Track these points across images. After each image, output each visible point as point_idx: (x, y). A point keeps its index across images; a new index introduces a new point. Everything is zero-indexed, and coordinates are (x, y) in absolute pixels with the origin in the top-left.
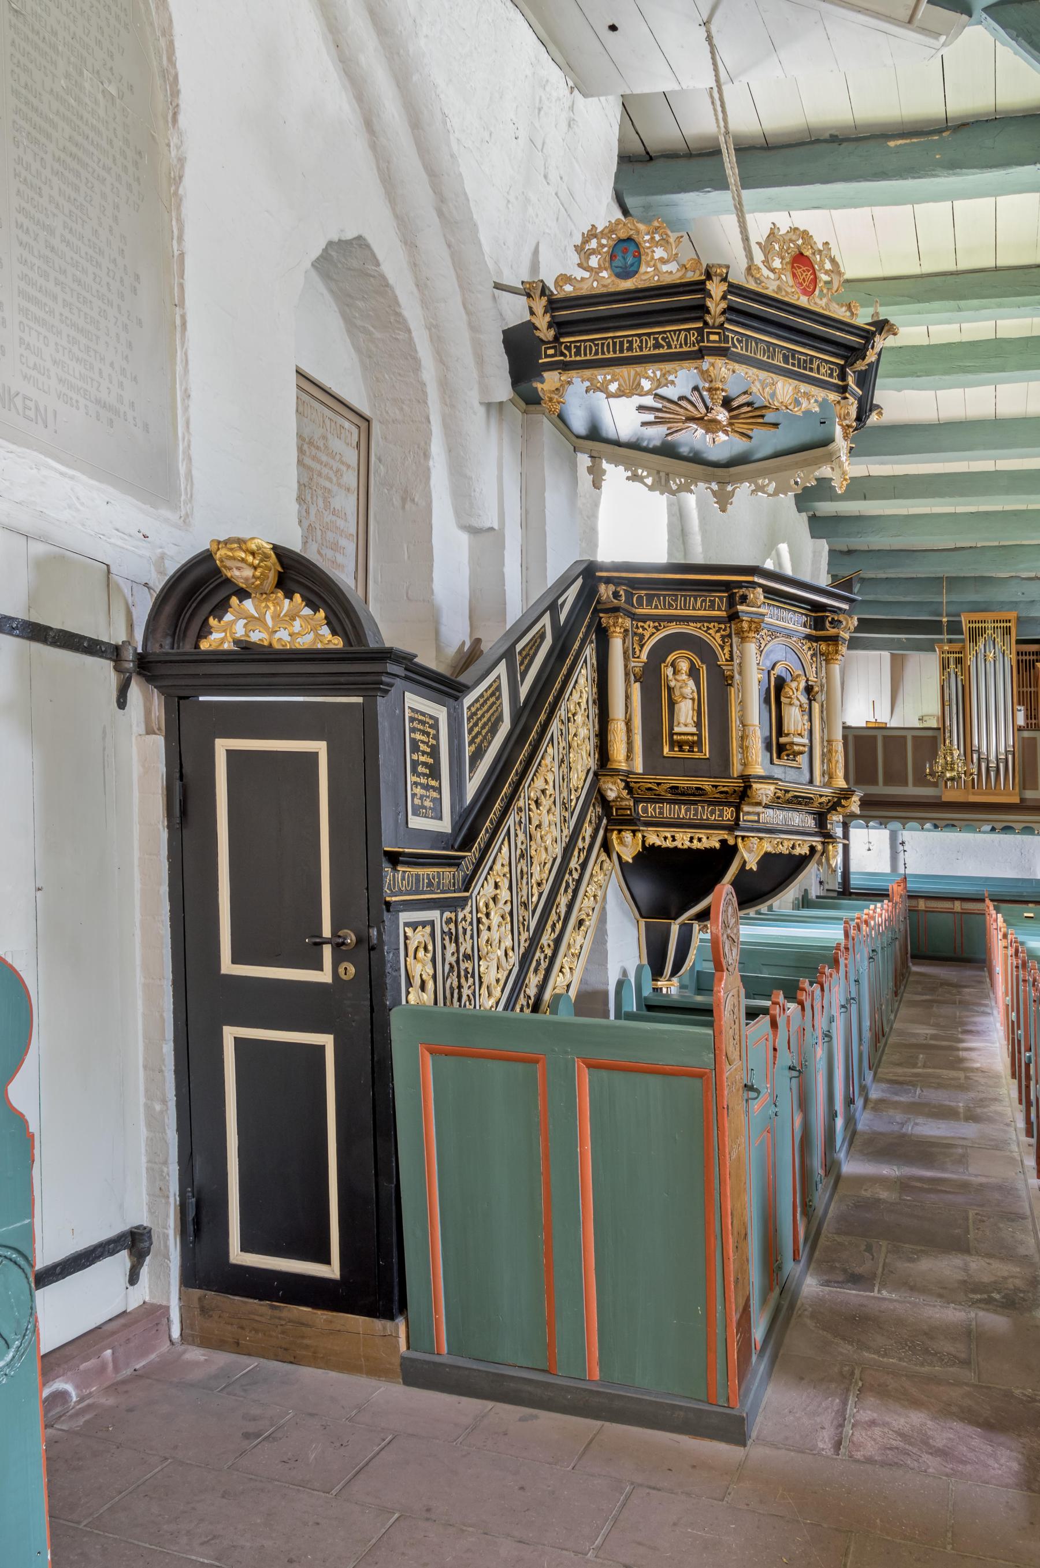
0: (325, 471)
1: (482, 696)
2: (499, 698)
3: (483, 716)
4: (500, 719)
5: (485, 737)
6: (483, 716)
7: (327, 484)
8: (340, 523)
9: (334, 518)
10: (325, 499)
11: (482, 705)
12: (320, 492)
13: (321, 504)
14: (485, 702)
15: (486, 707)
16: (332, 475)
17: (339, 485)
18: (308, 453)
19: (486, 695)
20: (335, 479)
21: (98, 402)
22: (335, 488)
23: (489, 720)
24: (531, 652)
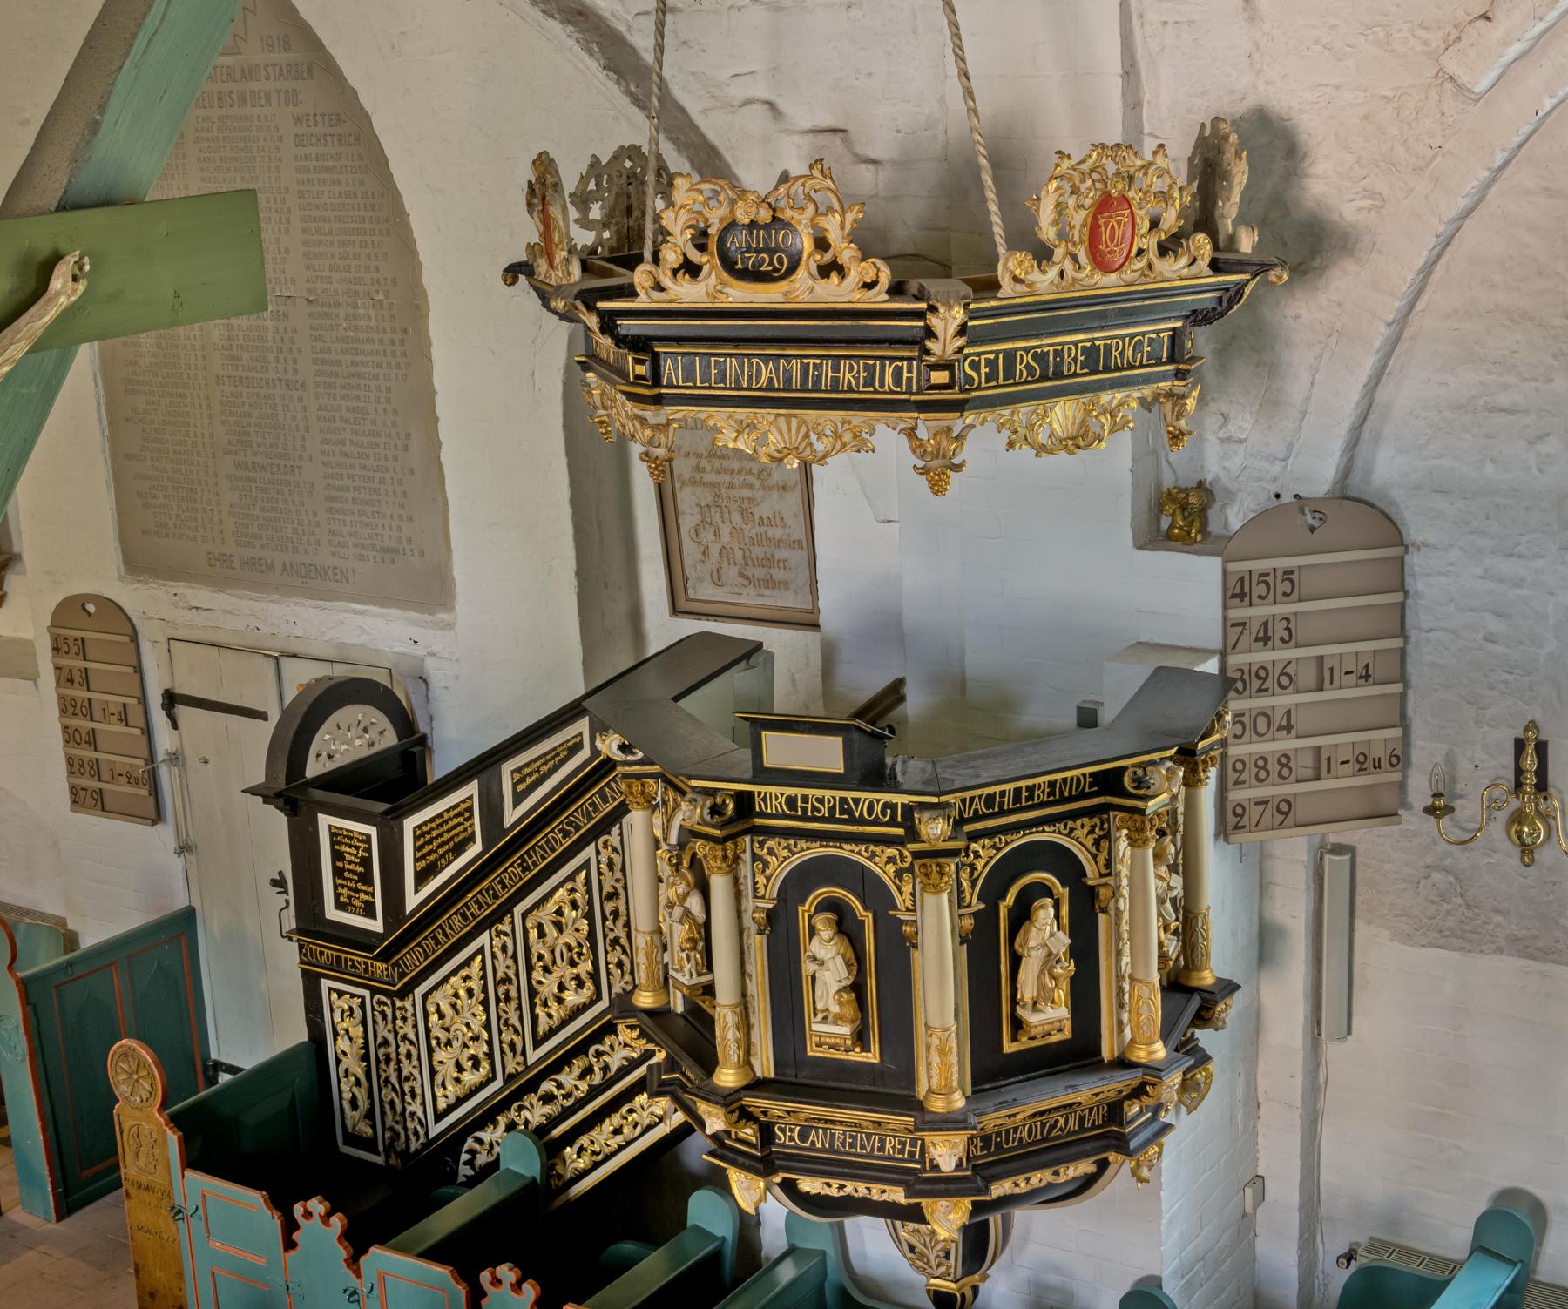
0: (738, 479)
1: (440, 815)
2: (471, 816)
3: (441, 835)
4: (471, 838)
5: (443, 856)
6: (441, 835)
7: (746, 493)
8: (776, 532)
9: (762, 530)
10: (743, 513)
11: (441, 825)
12: (732, 506)
13: (737, 518)
14: (446, 822)
15: (446, 828)
16: (751, 479)
17: (765, 487)
18: (708, 468)
19: (446, 816)
20: (757, 483)
21: (382, 549)
22: (759, 494)
23: (452, 839)
24: (545, 769)
